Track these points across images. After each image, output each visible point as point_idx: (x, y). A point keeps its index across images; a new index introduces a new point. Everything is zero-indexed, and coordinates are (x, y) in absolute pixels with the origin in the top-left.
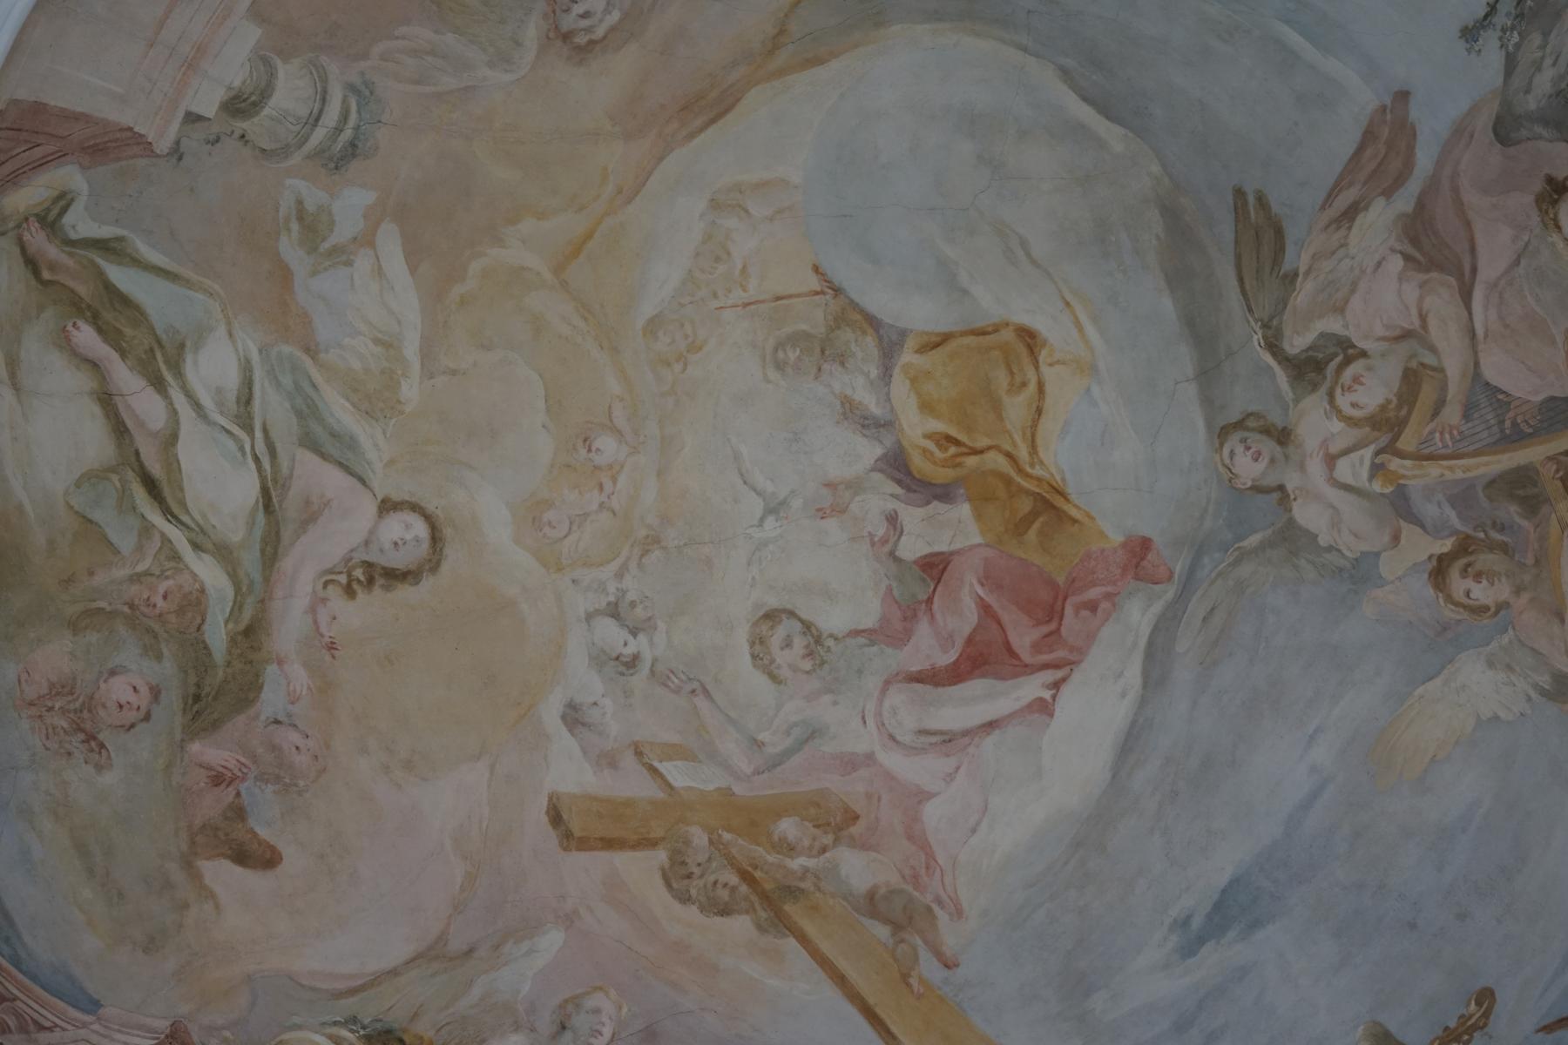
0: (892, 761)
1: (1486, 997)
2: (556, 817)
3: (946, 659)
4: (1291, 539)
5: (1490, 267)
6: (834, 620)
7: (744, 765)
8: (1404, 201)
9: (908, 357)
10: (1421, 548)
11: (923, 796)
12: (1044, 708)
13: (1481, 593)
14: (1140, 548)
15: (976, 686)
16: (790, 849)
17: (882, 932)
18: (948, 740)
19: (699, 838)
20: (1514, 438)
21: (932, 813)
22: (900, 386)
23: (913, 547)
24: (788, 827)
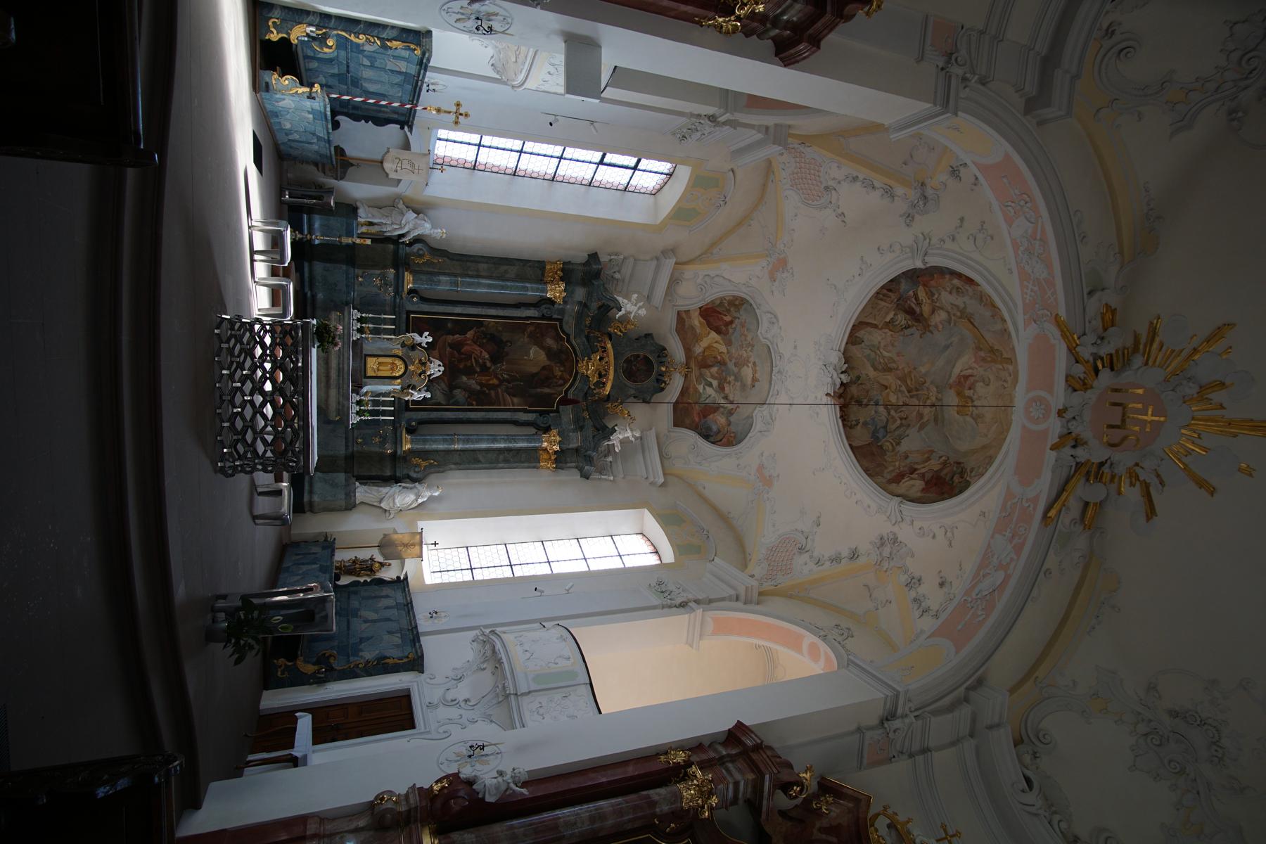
0: (977, 367)
1: (921, 337)
2: (1012, 362)
3: (970, 378)
4: (937, 387)
5: (915, 413)
6: (981, 384)
7: (993, 368)
8: (922, 421)
9: (969, 413)
10: (926, 385)
11: (975, 362)
12: (961, 371)
13: (921, 379)
14: (950, 388)
15: (967, 374)
16: (990, 357)
17: (981, 346)
18: (971, 368)
19: (999, 359)
20: (917, 395)
21: (973, 360)
22: (971, 410)
23: (972, 391)
24: (989, 359)
